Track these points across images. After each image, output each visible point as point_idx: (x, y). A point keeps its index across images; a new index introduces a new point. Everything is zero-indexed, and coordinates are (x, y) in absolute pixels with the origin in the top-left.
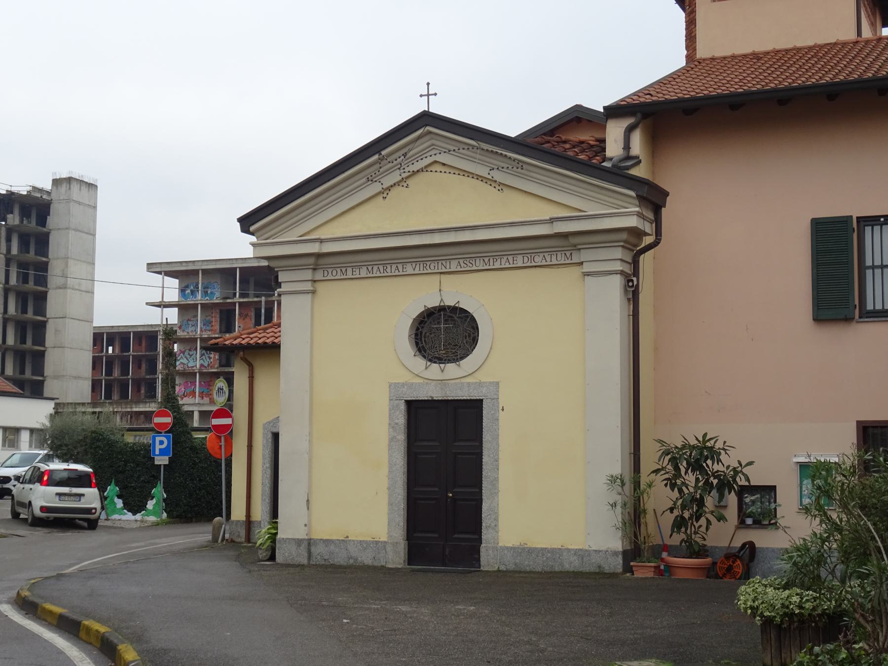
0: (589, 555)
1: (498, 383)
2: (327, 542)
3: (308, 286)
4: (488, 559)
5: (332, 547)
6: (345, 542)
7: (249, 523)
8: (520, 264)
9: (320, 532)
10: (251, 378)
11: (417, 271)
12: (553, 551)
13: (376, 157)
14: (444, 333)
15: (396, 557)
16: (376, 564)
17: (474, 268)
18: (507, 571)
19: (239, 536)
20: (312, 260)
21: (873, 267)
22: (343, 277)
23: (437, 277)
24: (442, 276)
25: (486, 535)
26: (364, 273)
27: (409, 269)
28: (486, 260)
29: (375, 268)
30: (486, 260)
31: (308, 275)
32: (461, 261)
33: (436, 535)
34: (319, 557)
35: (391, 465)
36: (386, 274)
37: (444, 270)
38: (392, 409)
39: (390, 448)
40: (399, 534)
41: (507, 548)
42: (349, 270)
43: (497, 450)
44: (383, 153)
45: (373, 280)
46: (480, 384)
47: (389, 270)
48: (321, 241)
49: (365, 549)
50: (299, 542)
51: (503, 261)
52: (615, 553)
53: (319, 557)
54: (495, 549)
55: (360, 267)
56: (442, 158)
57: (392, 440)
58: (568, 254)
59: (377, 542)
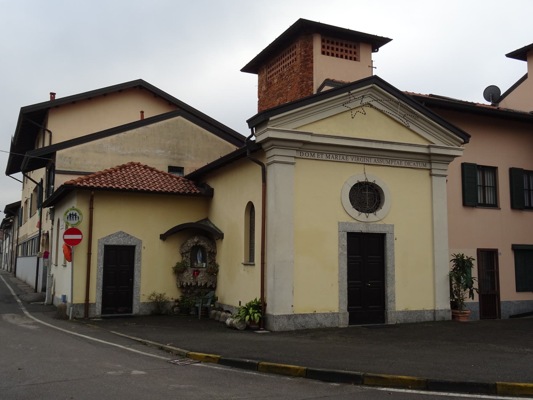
0: (438, 312)
1: (393, 225)
2: (304, 315)
3: (292, 160)
4: (391, 319)
5: (307, 319)
6: (314, 314)
7: (87, 305)
8: (404, 166)
9: (299, 310)
10: (91, 209)
11: (354, 161)
12: (420, 312)
13: (347, 93)
14: (367, 197)
15: (343, 322)
16: (333, 326)
17: (382, 164)
18: (401, 324)
19: (78, 314)
20: (300, 145)
21: (488, 186)
22: (312, 158)
23: (363, 166)
24: (365, 166)
25: (389, 305)
26: (324, 157)
27: (350, 159)
28: (388, 160)
29: (331, 156)
30: (388, 160)
31: (294, 153)
32: (376, 159)
33: (360, 307)
34: (299, 325)
35: (340, 268)
36: (337, 160)
37: (368, 163)
38: (340, 238)
39: (339, 258)
40: (345, 307)
41: (400, 312)
42: (316, 155)
43: (394, 260)
44: (352, 92)
45: (329, 162)
46: (385, 225)
47: (338, 158)
48: (311, 134)
49: (327, 318)
50: (289, 317)
51: (396, 163)
52: (449, 311)
53: (299, 325)
54: (395, 312)
55: (322, 154)
56: (374, 103)
57: (340, 254)
58: (424, 164)
59: (333, 313)
